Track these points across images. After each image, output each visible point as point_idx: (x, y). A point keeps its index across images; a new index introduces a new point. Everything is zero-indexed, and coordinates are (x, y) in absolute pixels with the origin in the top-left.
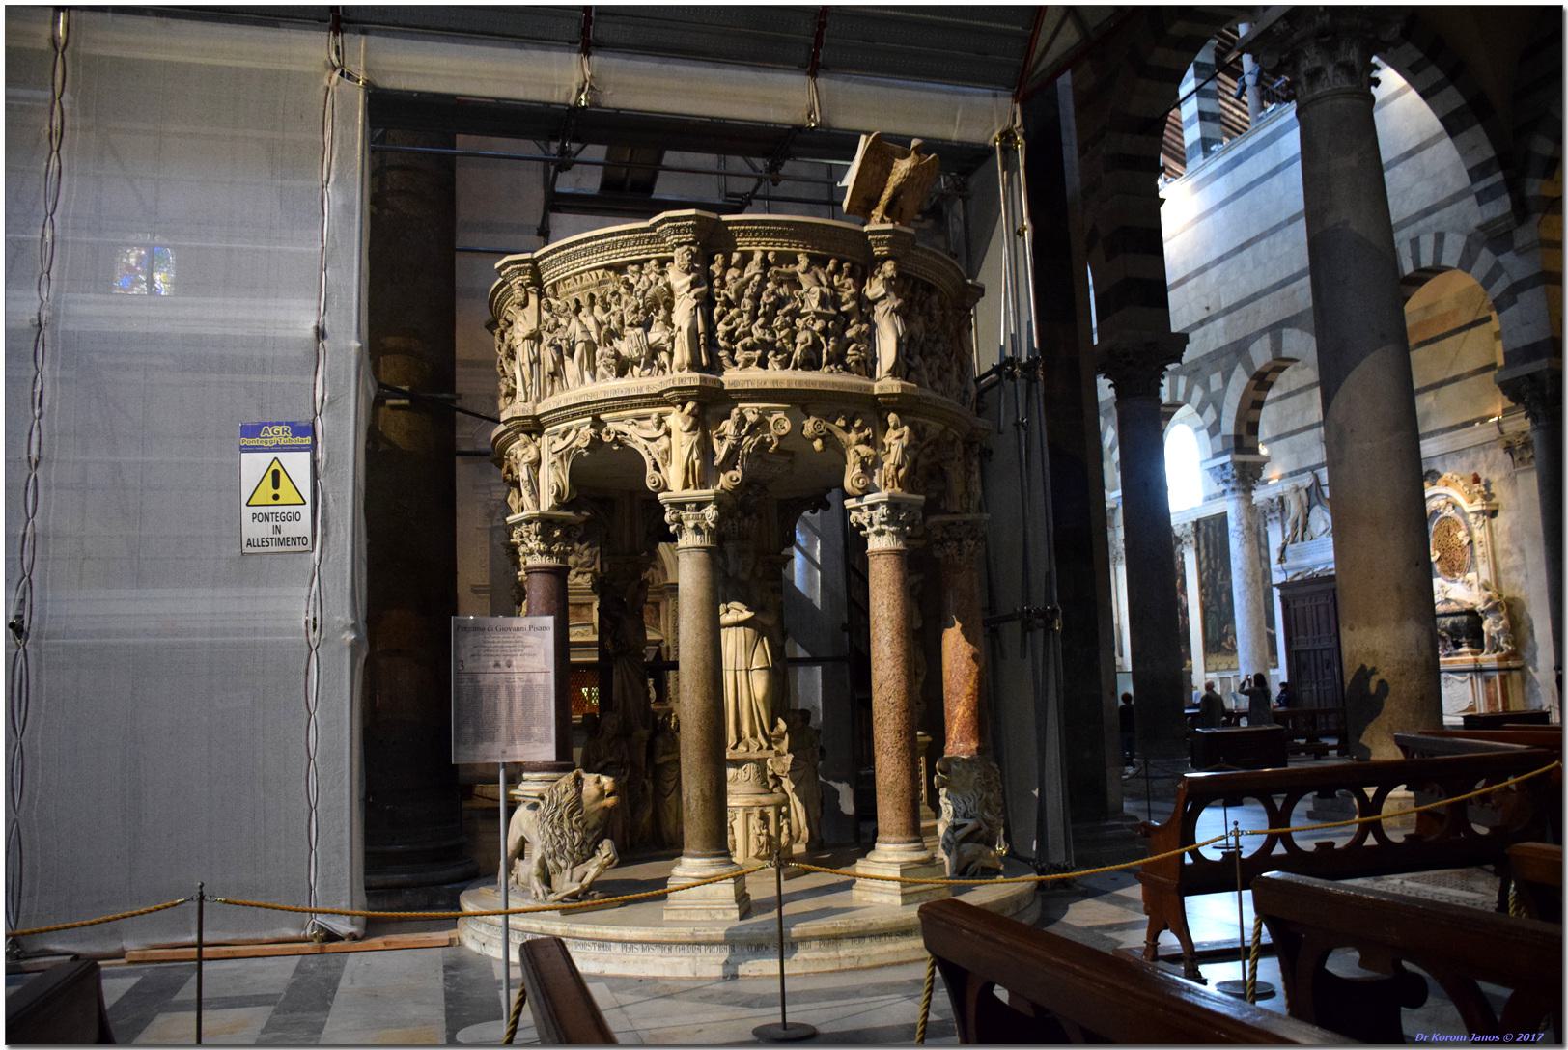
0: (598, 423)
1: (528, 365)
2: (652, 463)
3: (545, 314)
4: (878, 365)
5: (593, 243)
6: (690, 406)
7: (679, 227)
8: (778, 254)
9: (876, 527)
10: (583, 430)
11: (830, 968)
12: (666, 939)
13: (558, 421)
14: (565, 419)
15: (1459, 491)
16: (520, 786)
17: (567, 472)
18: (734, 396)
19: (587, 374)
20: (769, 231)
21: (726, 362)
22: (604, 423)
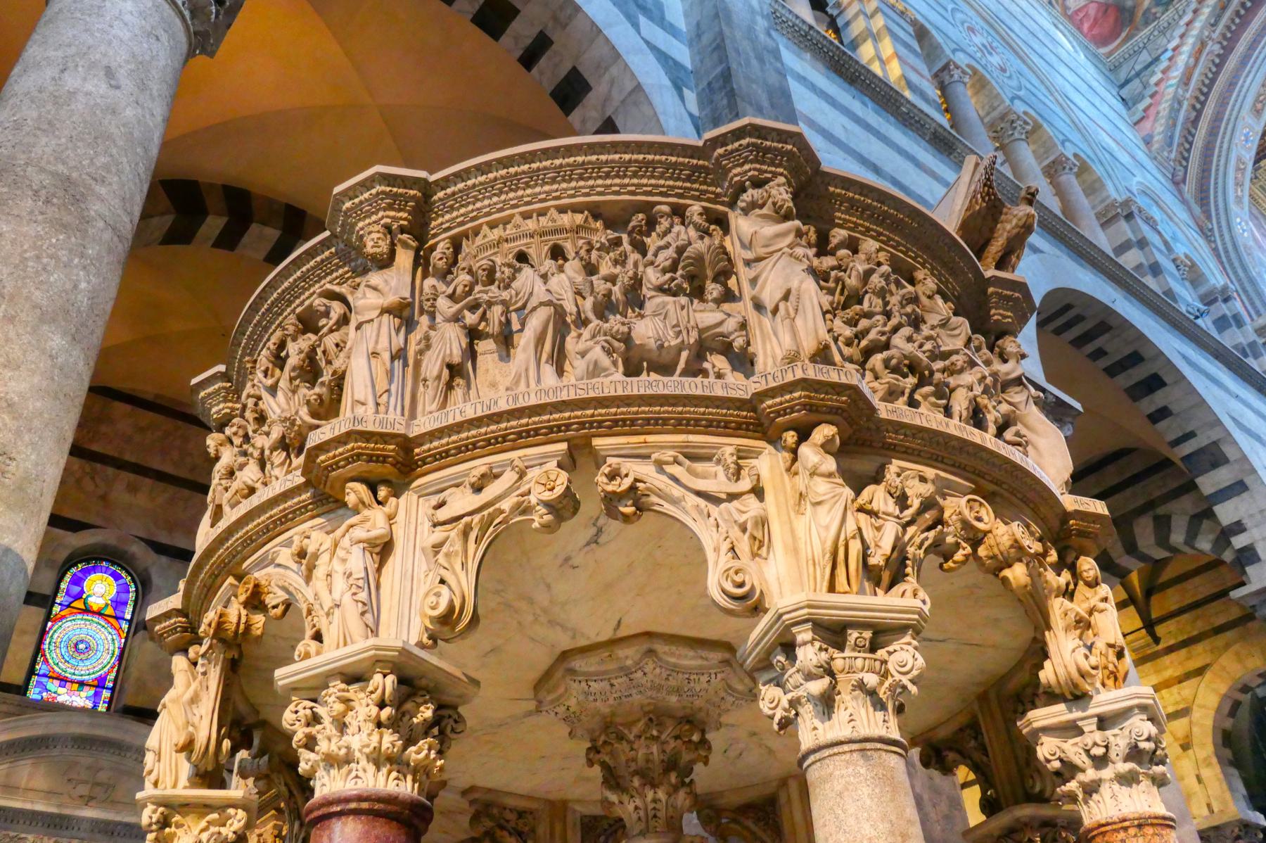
1: (386, 356)
2: (725, 546)
6: (824, 432)
13: (467, 451)
17: (473, 567)
18: (891, 438)
20: (886, 215)
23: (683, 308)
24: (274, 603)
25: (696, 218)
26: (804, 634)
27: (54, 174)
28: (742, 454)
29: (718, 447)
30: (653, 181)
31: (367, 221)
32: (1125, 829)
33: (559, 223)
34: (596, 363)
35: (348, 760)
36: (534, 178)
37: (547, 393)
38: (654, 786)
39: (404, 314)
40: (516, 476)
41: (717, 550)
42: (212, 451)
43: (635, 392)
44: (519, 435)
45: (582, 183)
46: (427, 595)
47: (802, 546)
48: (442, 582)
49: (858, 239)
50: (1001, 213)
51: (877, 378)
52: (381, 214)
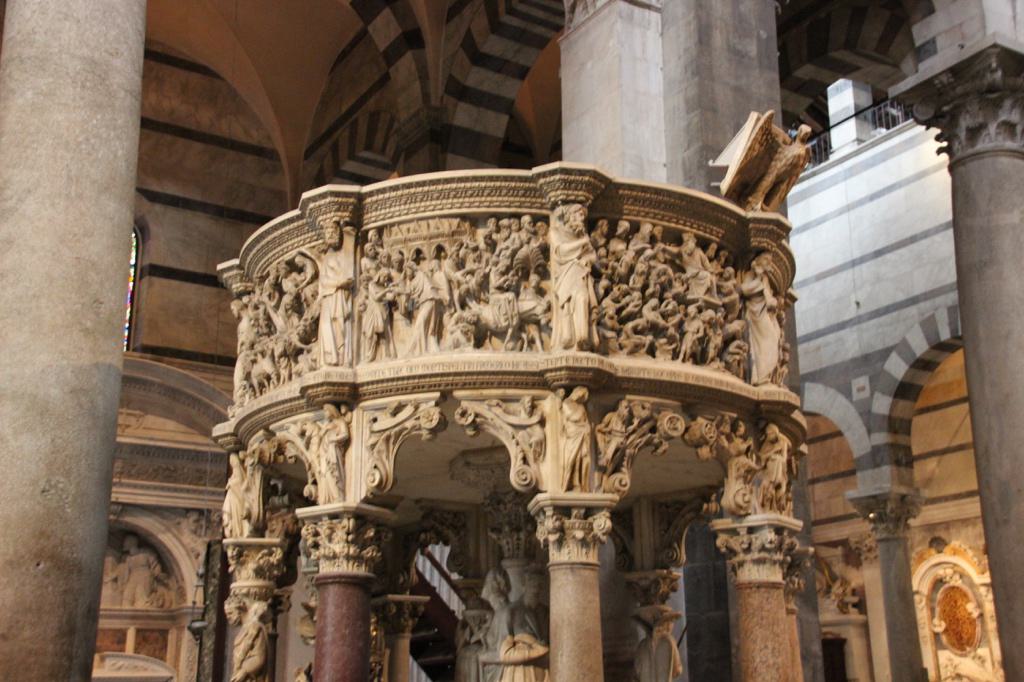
0: (446, 399)
1: (341, 320)
2: (520, 456)
3: (365, 262)
4: (754, 369)
5: (454, 185)
6: (578, 393)
7: (571, 182)
8: (666, 230)
9: (756, 555)
10: (423, 407)
14: (404, 391)
15: (969, 561)
17: (392, 457)
18: (625, 385)
19: (432, 340)
20: (660, 202)
21: (613, 344)
22: (458, 402)
23: (509, 302)
25: (527, 226)
27: (83, 59)
29: (523, 395)
30: (500, 199)
31: (325, 216)
32: (751, 588)
33: (441, 230)
34: (458, 340)
35: (335, 557)
36: (426, 196)
39: (349, 289)
40: (413, 409)
41: (516, 458)
42: (235, 312)
43: (475, 370)
45: (455, 200)
46: (368, 475)
47: (561, 454)
48: (376, 467)
50: (776, 152)
51: (628, 337)
52: (332, 214)
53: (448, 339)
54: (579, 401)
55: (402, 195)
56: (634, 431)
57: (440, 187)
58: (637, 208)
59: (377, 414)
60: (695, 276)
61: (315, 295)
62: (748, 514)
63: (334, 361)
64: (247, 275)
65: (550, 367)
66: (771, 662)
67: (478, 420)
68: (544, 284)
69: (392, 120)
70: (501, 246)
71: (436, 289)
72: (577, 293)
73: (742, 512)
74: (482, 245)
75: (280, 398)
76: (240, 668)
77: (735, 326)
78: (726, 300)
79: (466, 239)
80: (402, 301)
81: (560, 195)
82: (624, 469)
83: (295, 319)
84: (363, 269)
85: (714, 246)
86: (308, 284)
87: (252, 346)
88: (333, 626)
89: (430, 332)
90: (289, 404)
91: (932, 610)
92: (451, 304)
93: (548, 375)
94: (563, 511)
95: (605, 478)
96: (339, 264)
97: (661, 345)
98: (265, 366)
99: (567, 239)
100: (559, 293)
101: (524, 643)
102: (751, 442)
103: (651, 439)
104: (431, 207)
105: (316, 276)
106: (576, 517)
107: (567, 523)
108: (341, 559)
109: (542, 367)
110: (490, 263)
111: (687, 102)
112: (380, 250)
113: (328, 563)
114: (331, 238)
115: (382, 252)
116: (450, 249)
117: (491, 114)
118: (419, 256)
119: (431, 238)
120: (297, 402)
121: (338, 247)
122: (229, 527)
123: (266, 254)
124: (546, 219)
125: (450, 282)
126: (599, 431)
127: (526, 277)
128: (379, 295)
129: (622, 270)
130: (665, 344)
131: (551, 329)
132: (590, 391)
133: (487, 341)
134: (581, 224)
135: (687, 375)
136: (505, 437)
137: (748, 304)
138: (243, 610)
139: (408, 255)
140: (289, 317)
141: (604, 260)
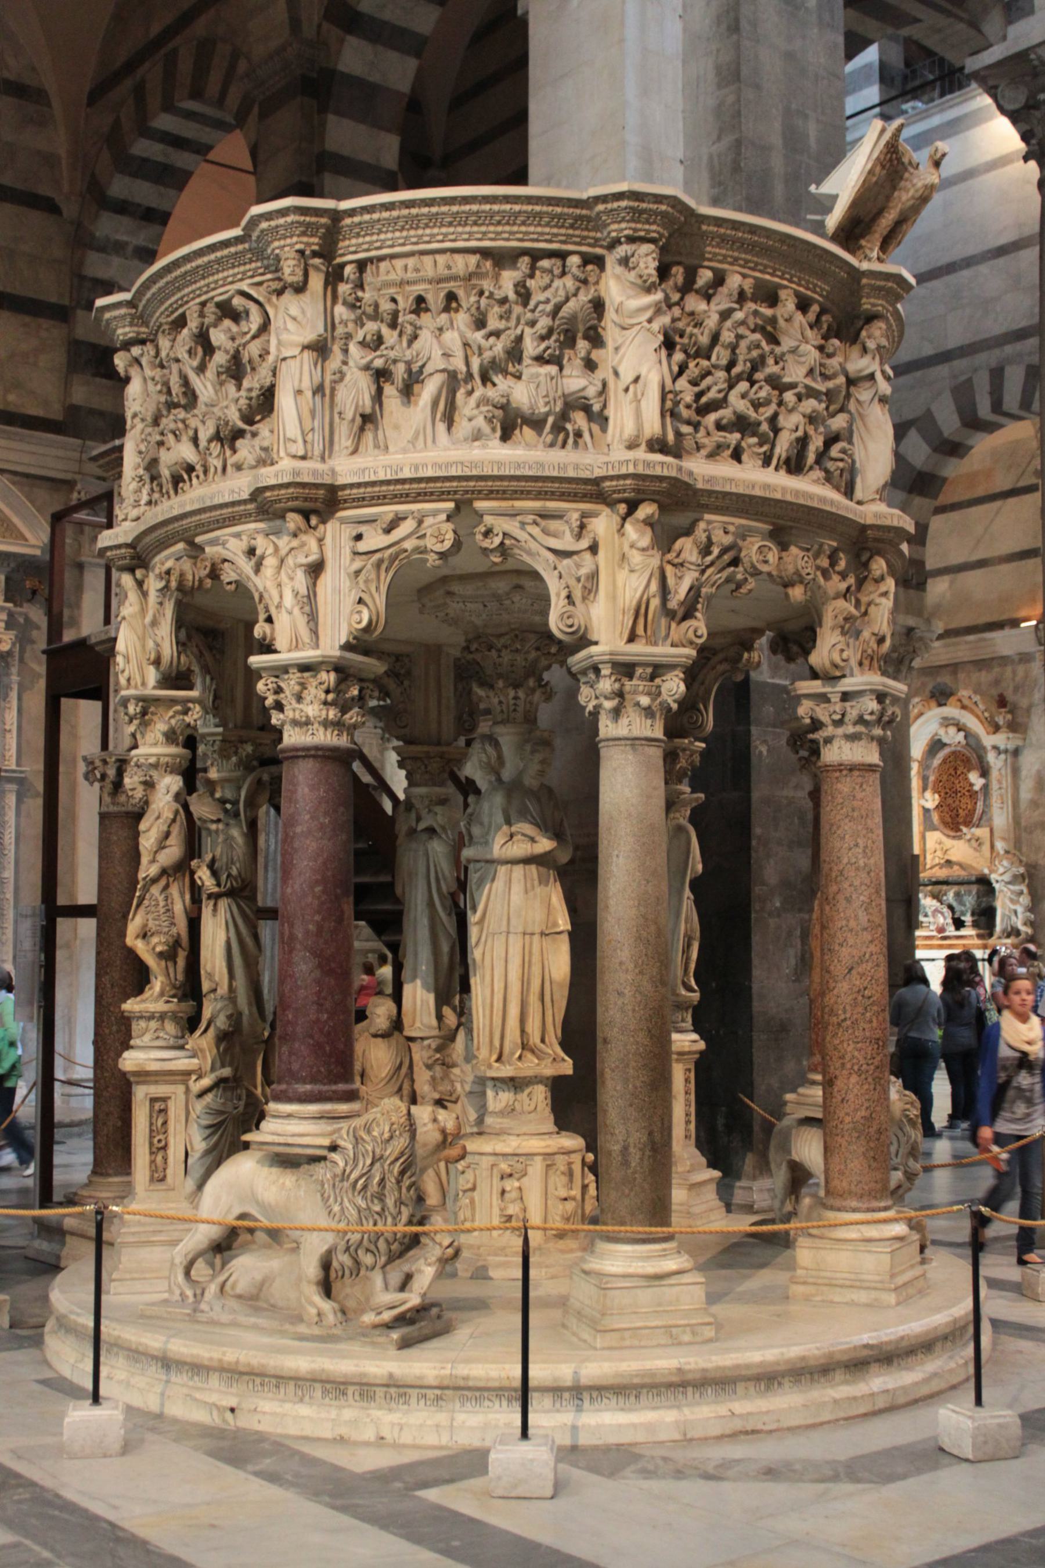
1: (309, 394)
2: (564, 593)
4: (858, 481)
5: (475, 207)
6: (646, 510)
8: (759, 284)
9: (851, 729)
10: (429, 521)
11: (862, 1410)
12: (636, 1381)
16: (264, 1125)
17: (384, 589)
18: (704, 500)
19: (441, 427)
20: (754, 245)
21: (688, 443)
23: (552, 378)
24: (228, 580)
25: (575, 270)
26: (606, 671)
28: (584, 515)
29: (567, 510)
30: (539, 229)
31: (282, 243)
33: (454, 271)
34: (479, 430)
35: (308, 723)
36: (433, 220)
37: (440, 467)
38: (516, 686)
39: (320, 349)
41: (558, 595)
42: (122, 373)
43: (507, 473)
44: (419, 494)
45: (475, 229)
46: (351, 613)
47: (620, 592)
48: (360, 601)
49: (724, 271)
50: (901, 178)
51: (708, 434)
52: (295, 239)
53: (463, 427)
54: (648, 522)
55: (398, 217)
56: (712, 564)
57: (455, 208)
58: (724, 252)
59: (363, 529)
60: (794, 351)
61: (264, 354)
62: (844, 676)
63: (301, 453)
64: (141, 317)
65: (611, 473)
66: (861, 863)
67: (507, 542)
68: (595, 355)
69: (235, 56)
70: (537, 297)
71: (446, 355)
72: (649, 371)
73: (838, 674)
74: (512, 296)
75: (217, 501)
76: (153, 861)
77: (838, 422)
78: (830, 384)
79: (487, 285)
80: (399, 371)
81: (625, 228)
82: (698, 615)
83: (231, 387)
84: (337, 321)
85: (815, 308)
86: (254, 337)
87: (156, 422)
88: (309, 812)
89: (439, 416)
90: (230, 510)
91: (925, 779)
92: (470, 376)
93: (608, 484)
94: (625, 669)
95: (673, 625)
96: (303, 312)
97: (749, 446)
98: (186, 452)
99: (631, 292)
100: (621, 370)
101: (524, 835)
102: (851, 580)
103: (734, 573)
104: (438, 237)
105: (265, 327)
106: (640, 678)
107: (629, 685)
108: (316, 725)
109: (598, 473)
110: (522, 321)
111: (718, 69)
112: (360, 294)
113: (297, 729)
114: (293, 274)
115: (367, 296)
116: (468, 300)
117: (393, 56)
118: (420, 304)
119: (439, 281)
120: (242, 508)
121: (300, 289)
122: (126, 674)
123: (179, 289)
124: (599, 262)
125: (466, 345)
126: (669, 562)
127: (570, 341)
128: (364, 361)
129: (704, 340)
130: (754, 445)
131: (606, 419)
132: (662, 508)
133: (517, 432)
134: (654, 273)
135: (784, 490)
136: (542, 563)
137: (852, 389)
138: (149, 785)
139: (405, 303)
140: (222, 384)
141: (680, 325)
